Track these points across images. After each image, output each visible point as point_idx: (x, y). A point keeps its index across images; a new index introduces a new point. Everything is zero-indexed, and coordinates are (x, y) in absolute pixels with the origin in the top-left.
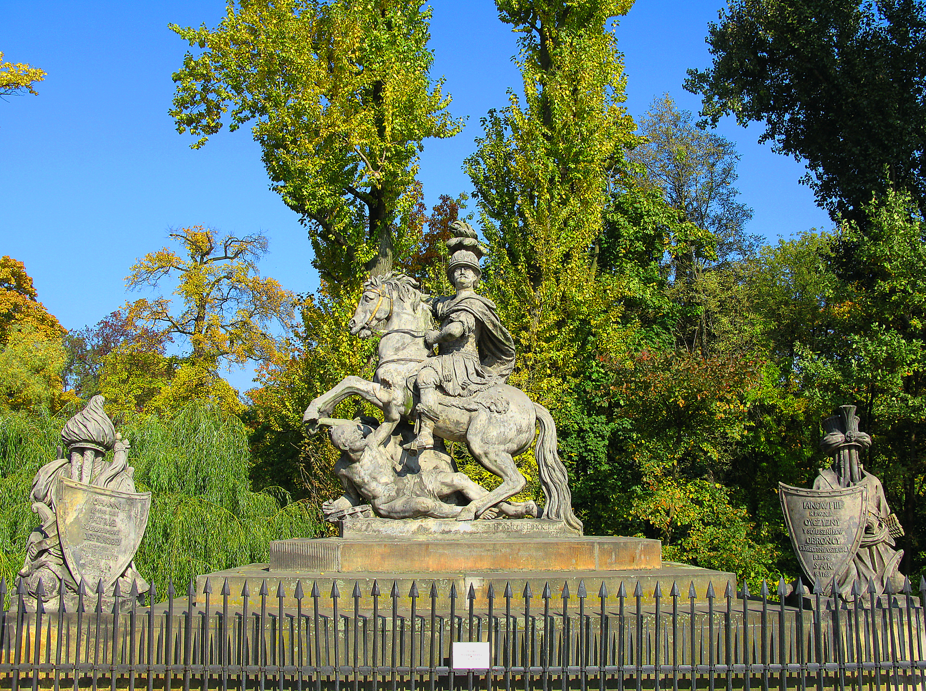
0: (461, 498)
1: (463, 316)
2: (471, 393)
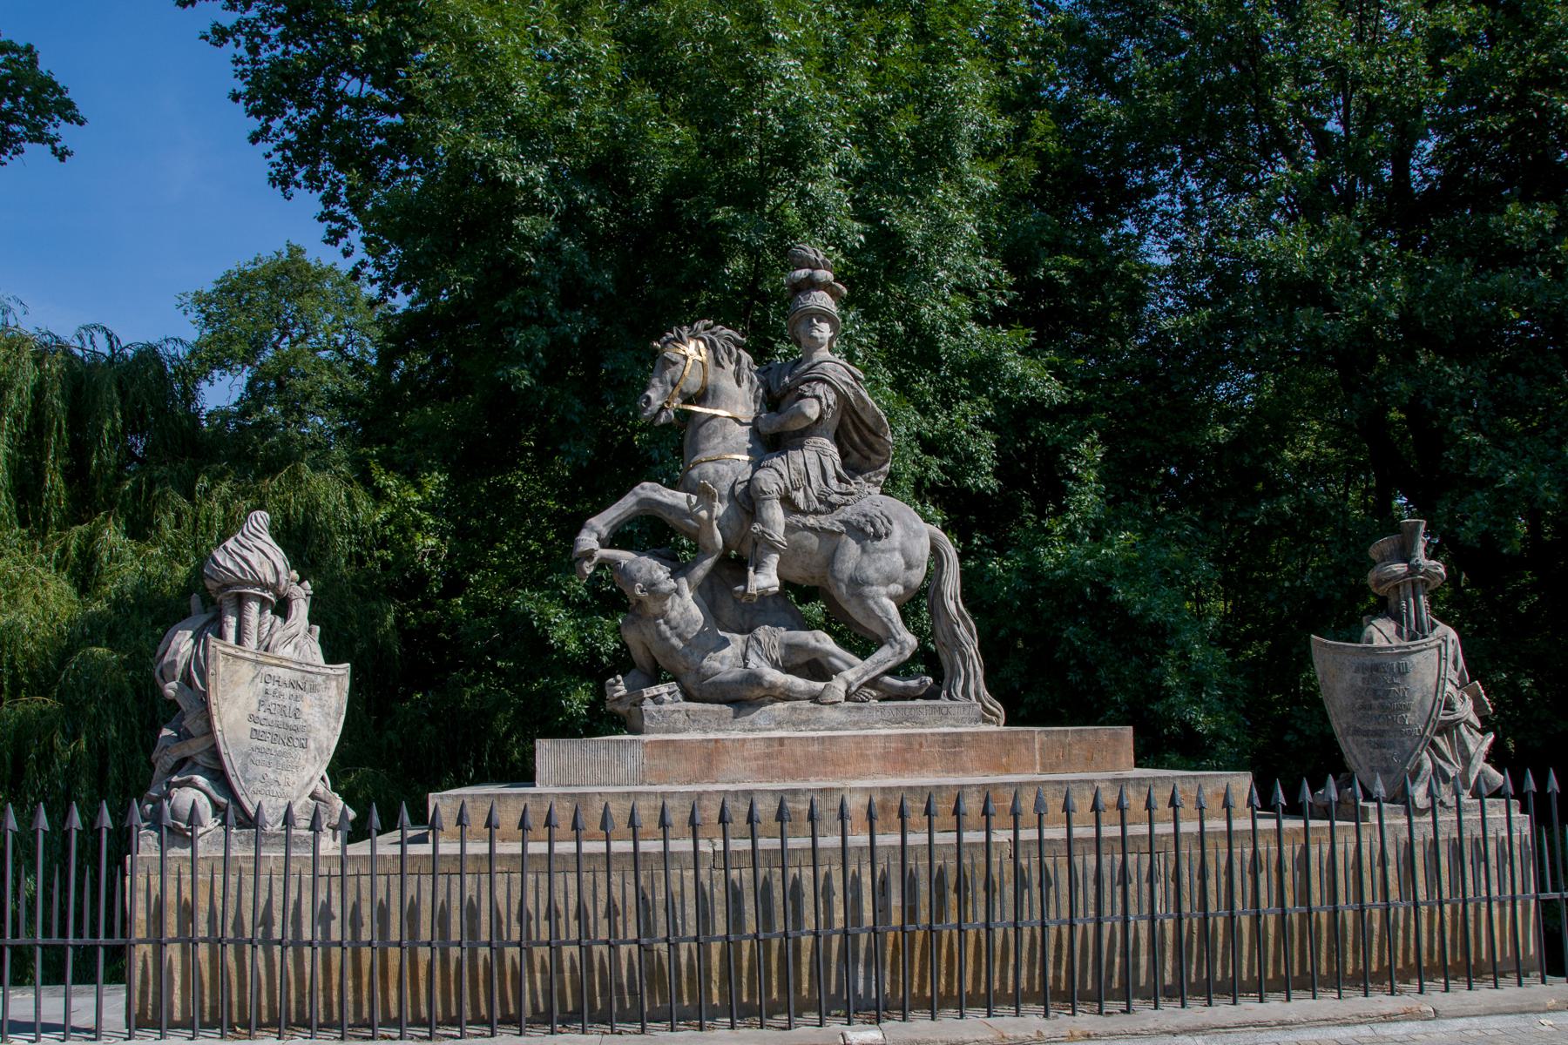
0: (818, 669)
1: (820, 389)
2: (832, 507)
